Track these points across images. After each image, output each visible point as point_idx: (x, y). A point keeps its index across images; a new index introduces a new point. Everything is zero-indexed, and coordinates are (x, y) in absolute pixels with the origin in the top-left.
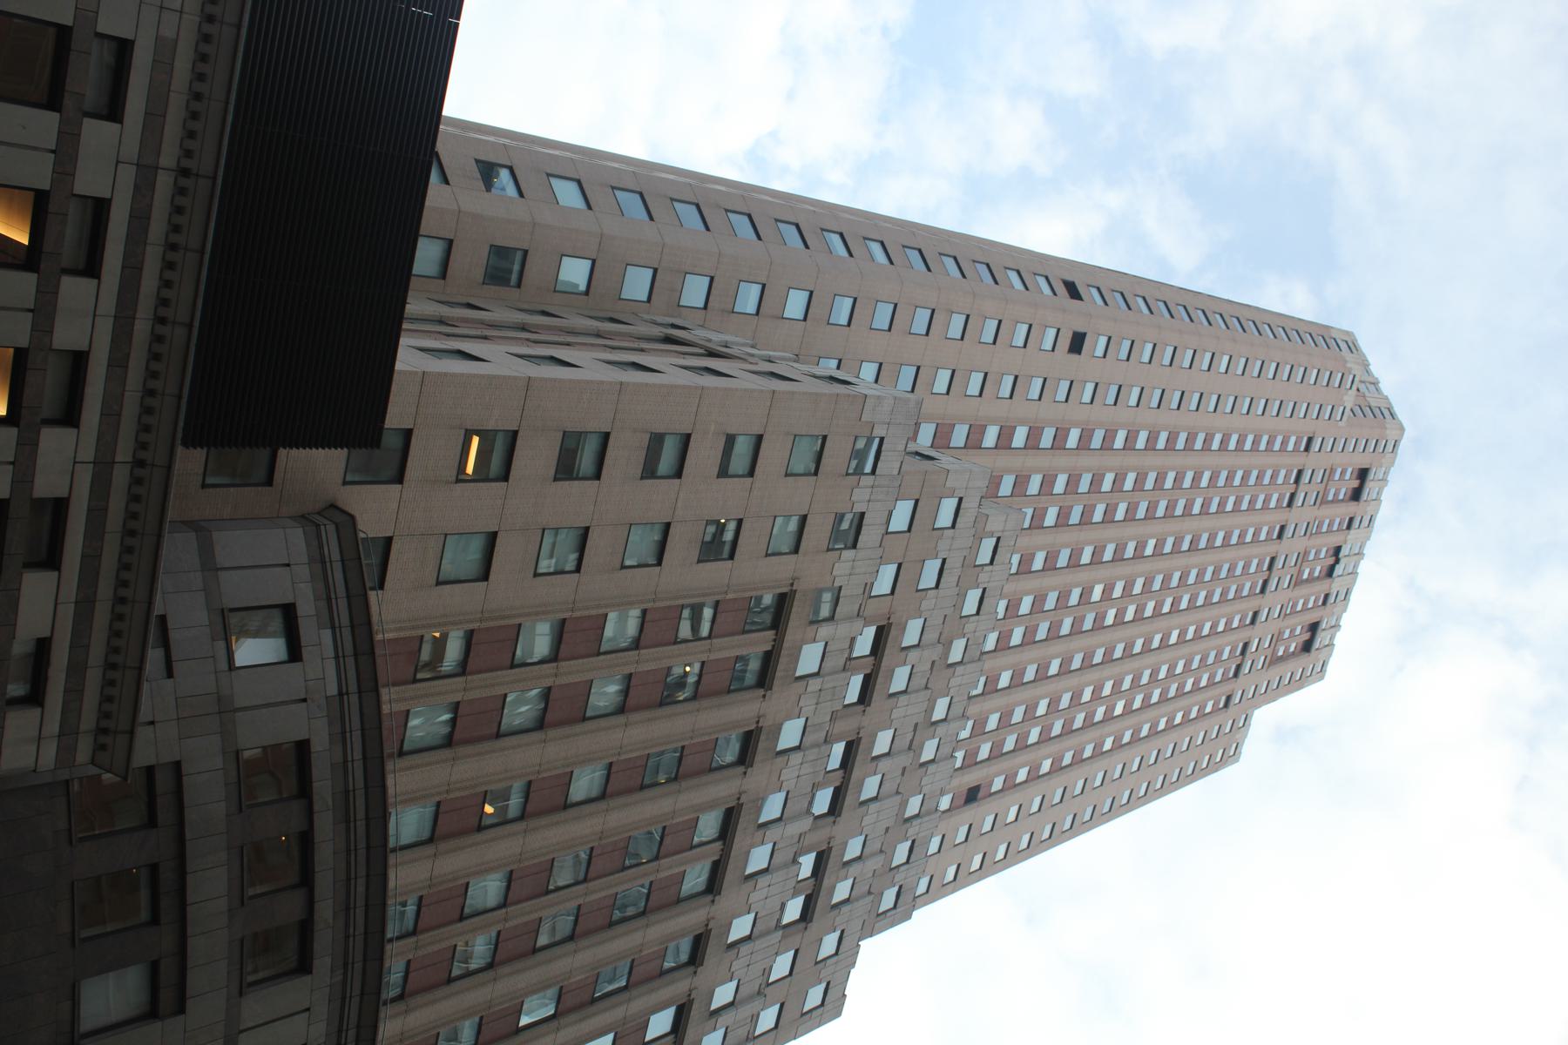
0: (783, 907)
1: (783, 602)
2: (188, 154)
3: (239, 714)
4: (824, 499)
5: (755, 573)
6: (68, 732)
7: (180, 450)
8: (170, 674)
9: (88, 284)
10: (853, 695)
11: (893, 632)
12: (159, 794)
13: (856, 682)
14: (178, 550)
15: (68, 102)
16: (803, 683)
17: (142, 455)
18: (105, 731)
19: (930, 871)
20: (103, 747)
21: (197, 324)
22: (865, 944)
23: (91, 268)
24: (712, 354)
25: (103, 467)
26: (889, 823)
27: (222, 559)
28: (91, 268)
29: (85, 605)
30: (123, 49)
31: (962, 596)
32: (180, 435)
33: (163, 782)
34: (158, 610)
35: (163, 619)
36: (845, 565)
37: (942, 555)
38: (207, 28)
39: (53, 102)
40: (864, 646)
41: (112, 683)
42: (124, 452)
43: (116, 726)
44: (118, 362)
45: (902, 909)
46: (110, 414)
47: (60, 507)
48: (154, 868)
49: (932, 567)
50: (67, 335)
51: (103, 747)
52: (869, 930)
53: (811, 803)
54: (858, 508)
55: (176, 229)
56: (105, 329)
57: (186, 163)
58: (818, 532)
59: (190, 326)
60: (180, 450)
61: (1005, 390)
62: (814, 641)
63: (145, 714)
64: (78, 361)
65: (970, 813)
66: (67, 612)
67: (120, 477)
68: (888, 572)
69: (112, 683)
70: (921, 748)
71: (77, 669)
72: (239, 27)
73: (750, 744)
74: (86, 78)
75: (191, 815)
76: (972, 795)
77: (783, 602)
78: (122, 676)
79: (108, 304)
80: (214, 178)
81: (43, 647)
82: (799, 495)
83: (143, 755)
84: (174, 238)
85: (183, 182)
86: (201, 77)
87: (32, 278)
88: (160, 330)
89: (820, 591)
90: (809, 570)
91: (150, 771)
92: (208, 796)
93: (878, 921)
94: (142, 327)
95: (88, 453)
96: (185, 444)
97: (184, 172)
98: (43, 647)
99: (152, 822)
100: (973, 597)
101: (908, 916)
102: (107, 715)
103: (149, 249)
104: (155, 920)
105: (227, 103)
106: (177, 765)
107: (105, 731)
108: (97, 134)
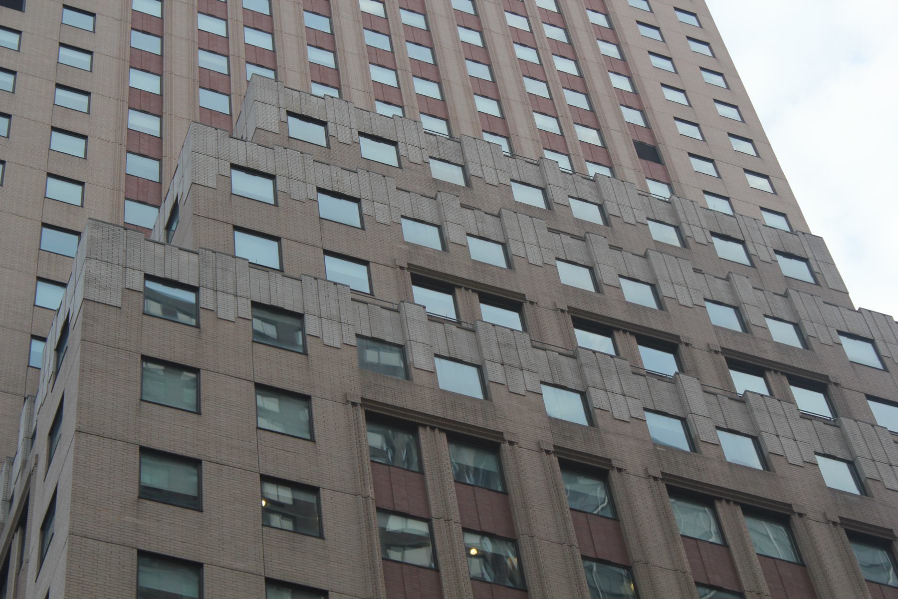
0: (805, 416)
1: (379, 417)
4: (231, 353)
5: (339, 455)
10: (510, 319)
11: (421, 262)
13: (491, 314)
16: (493, 388)
19: (756, 213)
22: (859, 301)
24: (22, 522)
26: (688, 267)
31: (371, 166)
36: (327, 330)
37: (313, 193)
40: (440, 303)
45: (810, 250)
49: (329, 207)
52: (838, 295)
53: (661, 377)
54: (246, 310)
58: (281, 369)
61: (78, 102)
62: (433, 373)
65: (674, 155)
68: (336, 269)
70: (581, 223)
73: (577, 463)
76: (649, 152)
77: (379, 417)
82: (226, 394)
89: (364, 365)
90: (332, 376)
93: (826, 284)
100: (372, 150)
101: (819, 242)
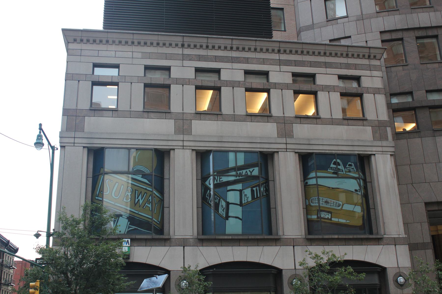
2: (177, 45)
3: (364, 13)
6: (370, 68)
7: (273, 39)
8: (350, 37)
9: (222, 72)
12: (391, 38)
14: (306, 37)
15: (167, 82)
17: (276, 51)
18: (369, 56)
20: (375, 57)
21: (231, 37)
23: (217, 71)
25: (281, 63)
27: (310, 23)
28: (217, 71)
29: (327, 65)
30: (147, 68)
32: (268, 39)
33: (387, 37)
34: (328, 42)
35: (331, 41)
38: (136, 43)
39: (168, 87)
41: (353, 55)
42: (276, 56)
43: (368, 53)
44: (247, 61)
46: (264, 62)
47: (295, 75)
48: (417, 38)
50: (240, 76)
51: (375, 57)
55: (201, 46)
56: (236, 66)
57: (180, 45)
59: (232, 39)
60: (273, 39)
63: (364, 44)
64: (247, 73)
66: (329, 70)
67: (284, 57)
69: (353, 55)
71: (348, 66)
72: (133, 34)
74: (157, 77)
75: (399, 27)
78: (350, 52)
79: (228, 65)
80: (183, 36)
81: (341, 77)
83: (379, 44)
84: (204, 47)
85: (186, 46)
86: (152, 44)
87: (223, 88)
88: (235, 48)
91: (383, 41)
92: (393, 21)
94: (235, 54)
95: (277, 68)
96: (271, 37)
97: (183, 45)
98: (341, 77)
99: (402, 39)
102: (364, 56)
103: (209, 54)
104: (436, 37)
105: (158, 35)
106: (381, 32)
107: (369, 56)
108: (175, 73)
